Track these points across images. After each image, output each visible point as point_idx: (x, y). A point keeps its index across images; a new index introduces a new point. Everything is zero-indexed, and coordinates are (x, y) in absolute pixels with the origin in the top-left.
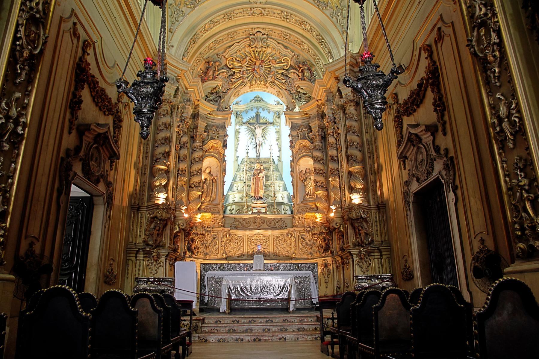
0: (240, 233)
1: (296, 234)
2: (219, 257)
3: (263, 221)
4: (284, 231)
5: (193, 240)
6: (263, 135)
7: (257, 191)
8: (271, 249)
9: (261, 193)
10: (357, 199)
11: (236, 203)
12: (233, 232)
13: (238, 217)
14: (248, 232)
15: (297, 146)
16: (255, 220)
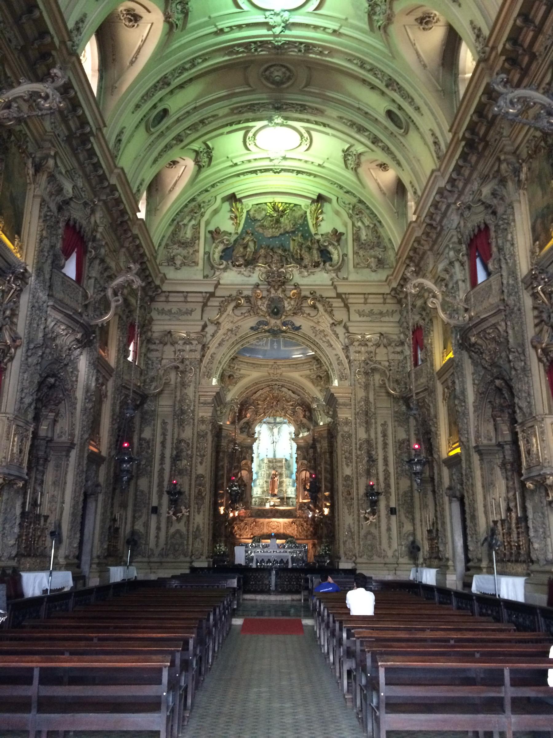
0: (262, 520)
1: (298, 523)
2: (249, 536)
3: (277, 511)
4: (291, 520)
5: (234, 528)
6: (279, 432)
7: (273, 490)
8: (282, 531)
9: (276, 491)
10: (326, 511)
11: (258, 497)
12: (257, 520)
13: (260, 508)
14: (267, 520)
15: (300, 463)
16: (271, 511)
